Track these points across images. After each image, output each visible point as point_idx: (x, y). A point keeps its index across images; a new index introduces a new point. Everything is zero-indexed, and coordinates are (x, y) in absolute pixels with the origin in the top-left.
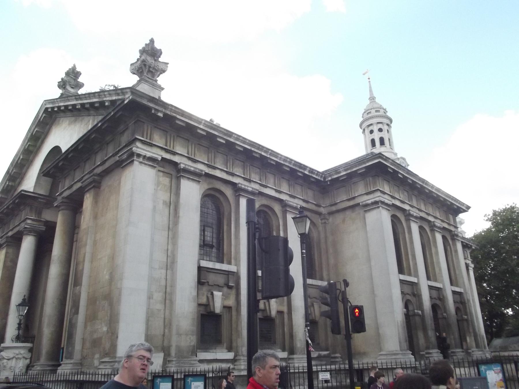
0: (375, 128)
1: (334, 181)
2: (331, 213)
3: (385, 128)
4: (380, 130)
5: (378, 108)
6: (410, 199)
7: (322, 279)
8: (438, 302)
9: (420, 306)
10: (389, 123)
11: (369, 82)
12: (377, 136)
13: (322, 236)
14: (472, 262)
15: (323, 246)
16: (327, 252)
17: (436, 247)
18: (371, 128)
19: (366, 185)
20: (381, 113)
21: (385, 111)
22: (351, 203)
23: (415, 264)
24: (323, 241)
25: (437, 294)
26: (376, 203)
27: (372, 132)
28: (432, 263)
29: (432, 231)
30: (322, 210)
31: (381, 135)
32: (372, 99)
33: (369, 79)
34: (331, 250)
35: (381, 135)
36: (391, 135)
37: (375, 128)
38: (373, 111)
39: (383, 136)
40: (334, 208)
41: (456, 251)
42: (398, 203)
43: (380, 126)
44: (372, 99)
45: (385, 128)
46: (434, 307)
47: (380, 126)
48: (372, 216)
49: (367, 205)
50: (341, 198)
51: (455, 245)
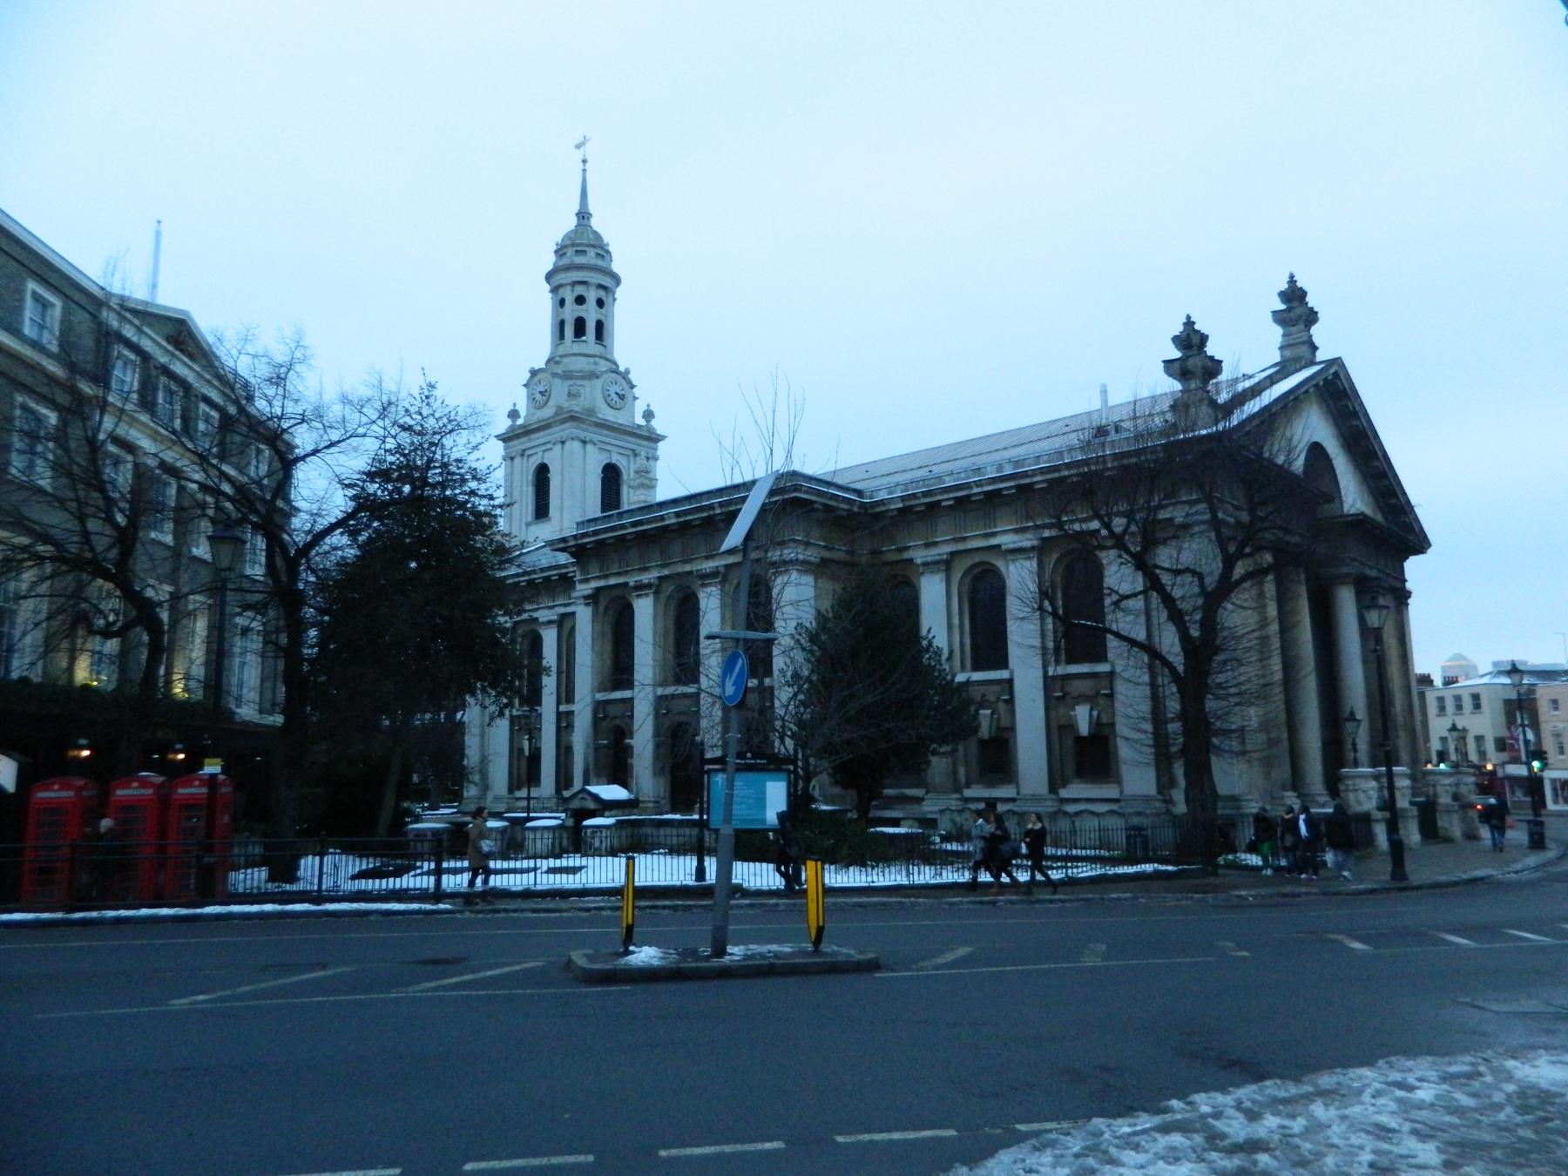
3: (592, 296)
4: (580, 300)
10: (607, 282)
12: (571, 312)
20: (590, 258)
27: (562, 302)
31: (581, 311)
32: (583, 216)
33: (584, 161)
35: (581, 311)
38: (570, 252)
39: (582, 314)
43: (580, 290)
44: (583, 216)
47: (580, 290)
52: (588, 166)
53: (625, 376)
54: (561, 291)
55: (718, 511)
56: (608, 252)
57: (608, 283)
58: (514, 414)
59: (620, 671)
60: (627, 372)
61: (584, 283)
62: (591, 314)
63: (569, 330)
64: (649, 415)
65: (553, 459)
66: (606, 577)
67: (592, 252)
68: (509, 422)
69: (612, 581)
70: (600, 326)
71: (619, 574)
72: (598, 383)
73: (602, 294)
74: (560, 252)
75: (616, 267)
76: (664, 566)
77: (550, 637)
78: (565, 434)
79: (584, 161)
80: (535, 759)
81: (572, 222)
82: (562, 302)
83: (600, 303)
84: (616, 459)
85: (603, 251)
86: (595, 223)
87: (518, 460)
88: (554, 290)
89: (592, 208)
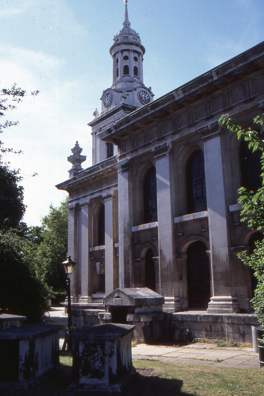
4: (126, 58)
10: (140, 50)
11: (126, 5)
31: (126, 63)
32: (127, 24)
35: (126, 63)
43: (126, 54)
44: (127, 24)
45: (132, 56)
47: (126, 54)
52: (127, 4)
53: (149, 90)
54: (117, 55)
55: (215, 78)
56: (138, 37)
57: (140, 51)
59: (146, 209)
60: (150, 88)
61: (128, 50)
62: (132, 64)
63: (121, 72)
66: (136, 150)
67: (131, 37)
69: (140, 152)
70: (136, 69)
71: (145, 146)
72: (136, 92)
73: (136, 55)
74: (116, 39)
75: (143, 44)
76: (174, 134)
77: (108, 205)
80: (102, 277)
83: (136, 59)
85: (137, 37)
88: (114, 56)
89: (130, 20)
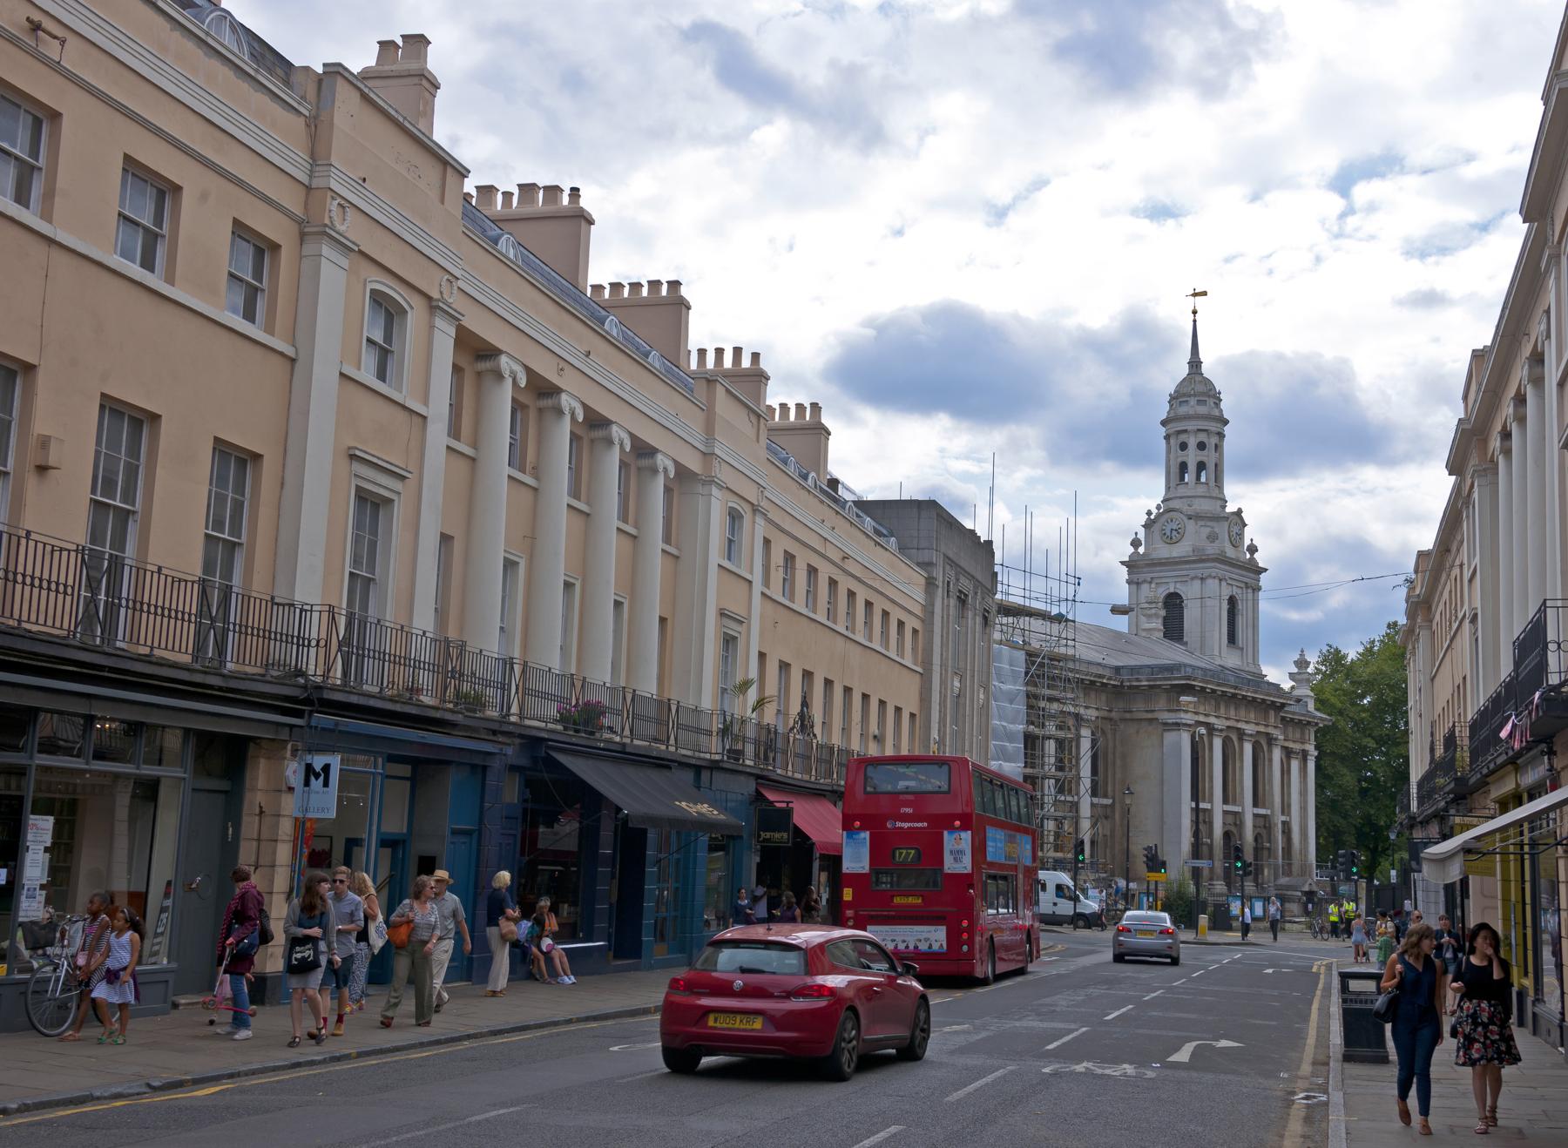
0: (1192, 442)
1: (1130, 687)
2: (1124, 720)
4: (1202, 446)
5: (1203, 394)
6: (1217, 708)
7: (1105, 796)
8: (1233, 829)
9: (1210, 835)
13: (1111, 745)
14: (1317, 748)
15: (1110, 756)
16: (1114, 763)
17: (1242, 761)
18: (1183, 437)
19: (1169, 700)
21: (1217, 398)
22: (1149, 716)
23: (1211, 788)
24: (1110, 750)
25: (1235, 819)
26: (1177, 724)
28: (1234, 780)
29: (1241, 740)
30: (1113, 715)
32: (1195, 363)
33: (1195, 312)
34: (1118, 762)
36: (1221, 455)
37: (1192, 442)
39: (1204, 459)
40: (1128, 716)
41: (1271, 760)
42: (1202, 718)
43: (1202, 437)
44: (1195, 363)
46: (1227, 835)
47: (1202, 437)
48: (1170, 737)
49: (1166, 724)
50: (1139, 706)
51: (1270, 752)
58: (1136, 543)
62: (1209, 457)
64: (1253, 549)
65: (1190, 591)
68: (1132, 550)
78: (1206, 572)
79: (1195, 312)
81: (1183, 370)
82: (1184, 446)
84: (1236, 591)
86: (1206, 369)
87: (1145, 587)
